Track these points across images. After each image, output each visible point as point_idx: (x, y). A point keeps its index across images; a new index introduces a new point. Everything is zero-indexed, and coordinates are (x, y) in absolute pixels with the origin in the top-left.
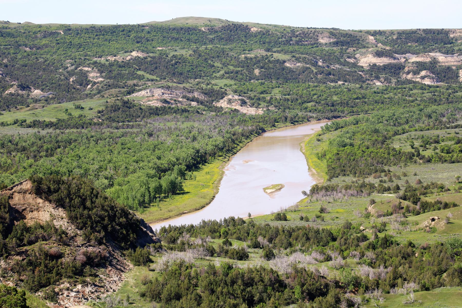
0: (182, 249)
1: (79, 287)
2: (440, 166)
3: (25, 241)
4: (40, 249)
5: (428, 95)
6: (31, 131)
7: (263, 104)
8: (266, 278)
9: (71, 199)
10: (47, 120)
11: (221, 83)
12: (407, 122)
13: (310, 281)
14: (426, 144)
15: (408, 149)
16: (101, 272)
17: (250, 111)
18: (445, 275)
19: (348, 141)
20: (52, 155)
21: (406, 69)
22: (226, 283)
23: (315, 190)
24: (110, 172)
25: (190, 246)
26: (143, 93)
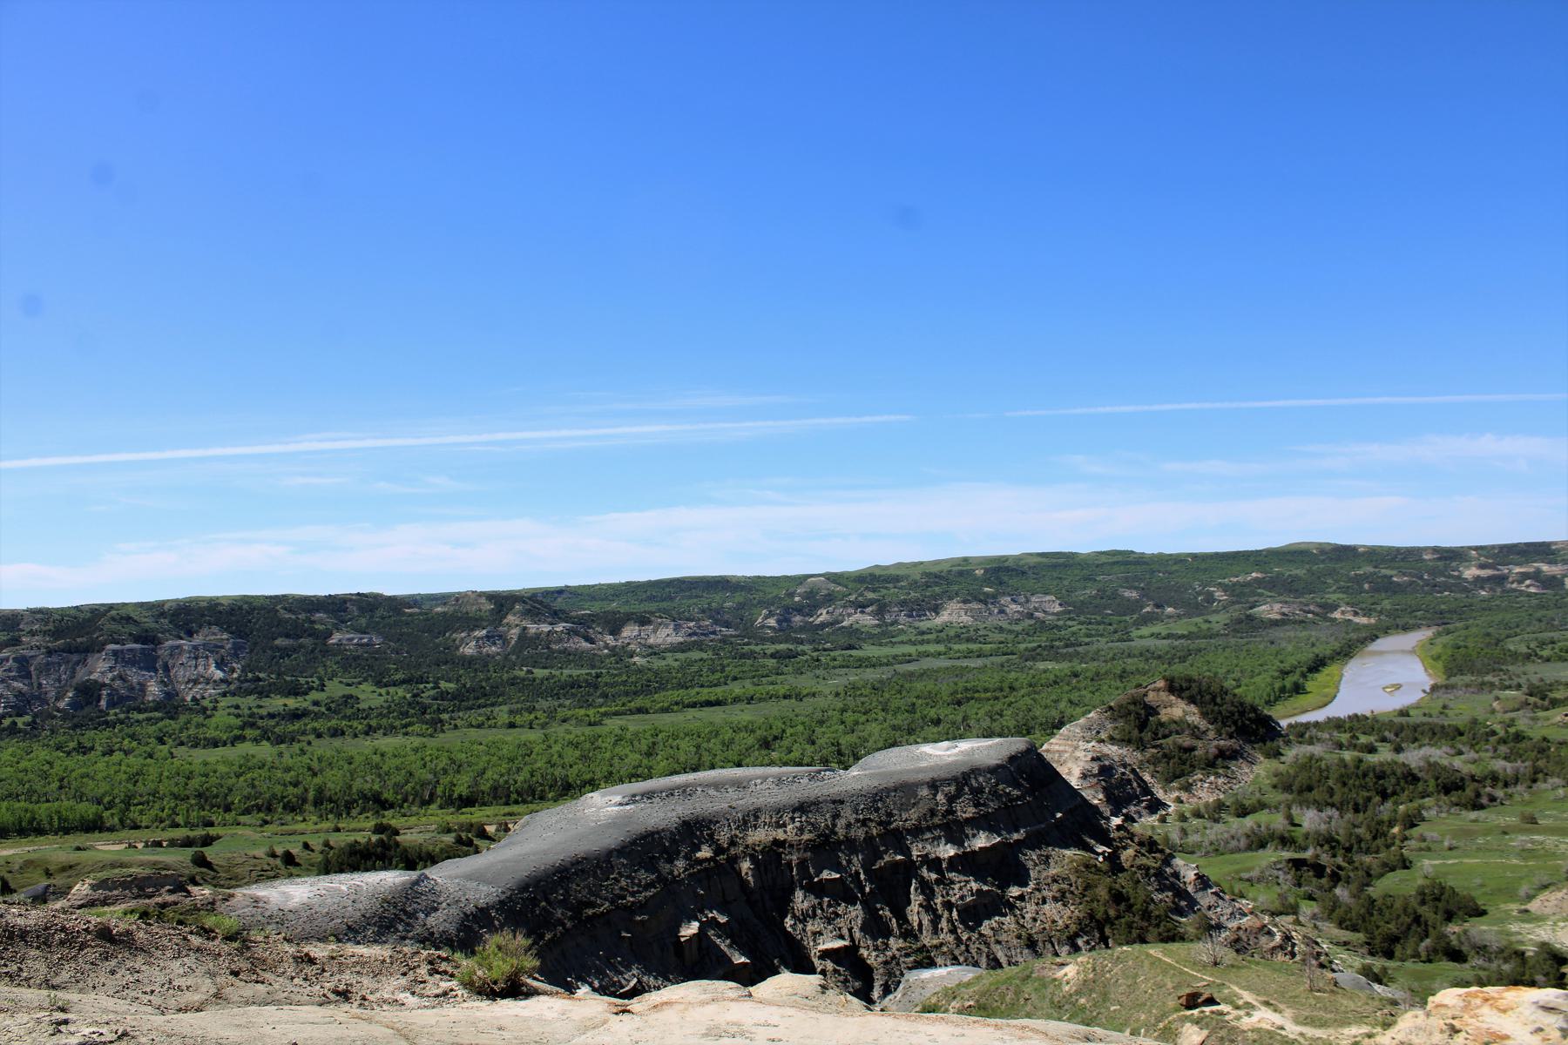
0: (1311, 742)
1: (1212, 778)
2: (1560, 665)
3: (1160, 736)
4: (1175, 743)
5: (1534, 602)
6: (1165, 641)
7: (1374, 614)
8: (1399, 772)
9: (1202, 697)
10: (1180, 632)
11: (1334, 597)
12: (1518, 626)
13: (1444, 775)
14: (1542, 644)
15: (1523, 649)
16: (1233, 765)
17: (1363, 620)
19: (1462, 644)
20: (1184, 662)
21: (1510, 579)
22: (1357, 776)
23: (1434, 688)
24: (1237, 675)
25: (1318, 740)
26: (1264, 607)
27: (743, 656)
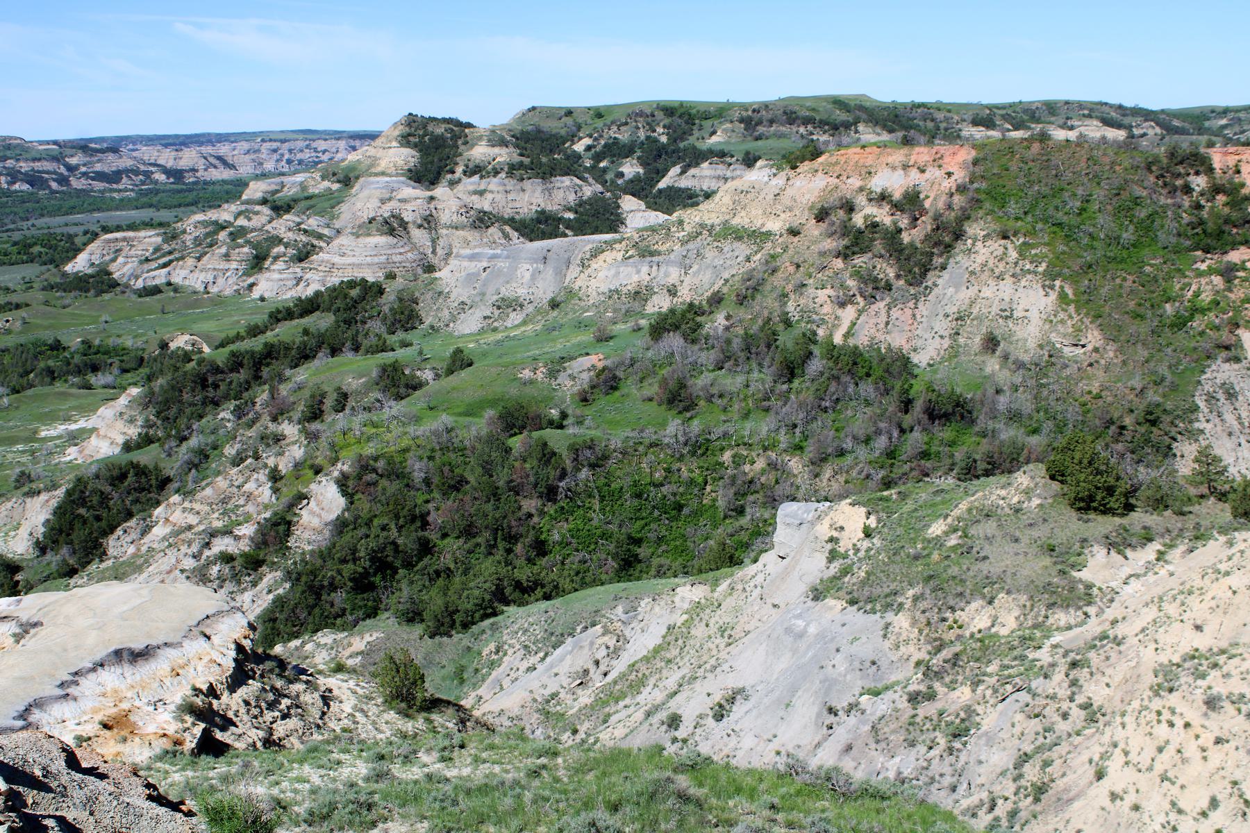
18: (32, 375)
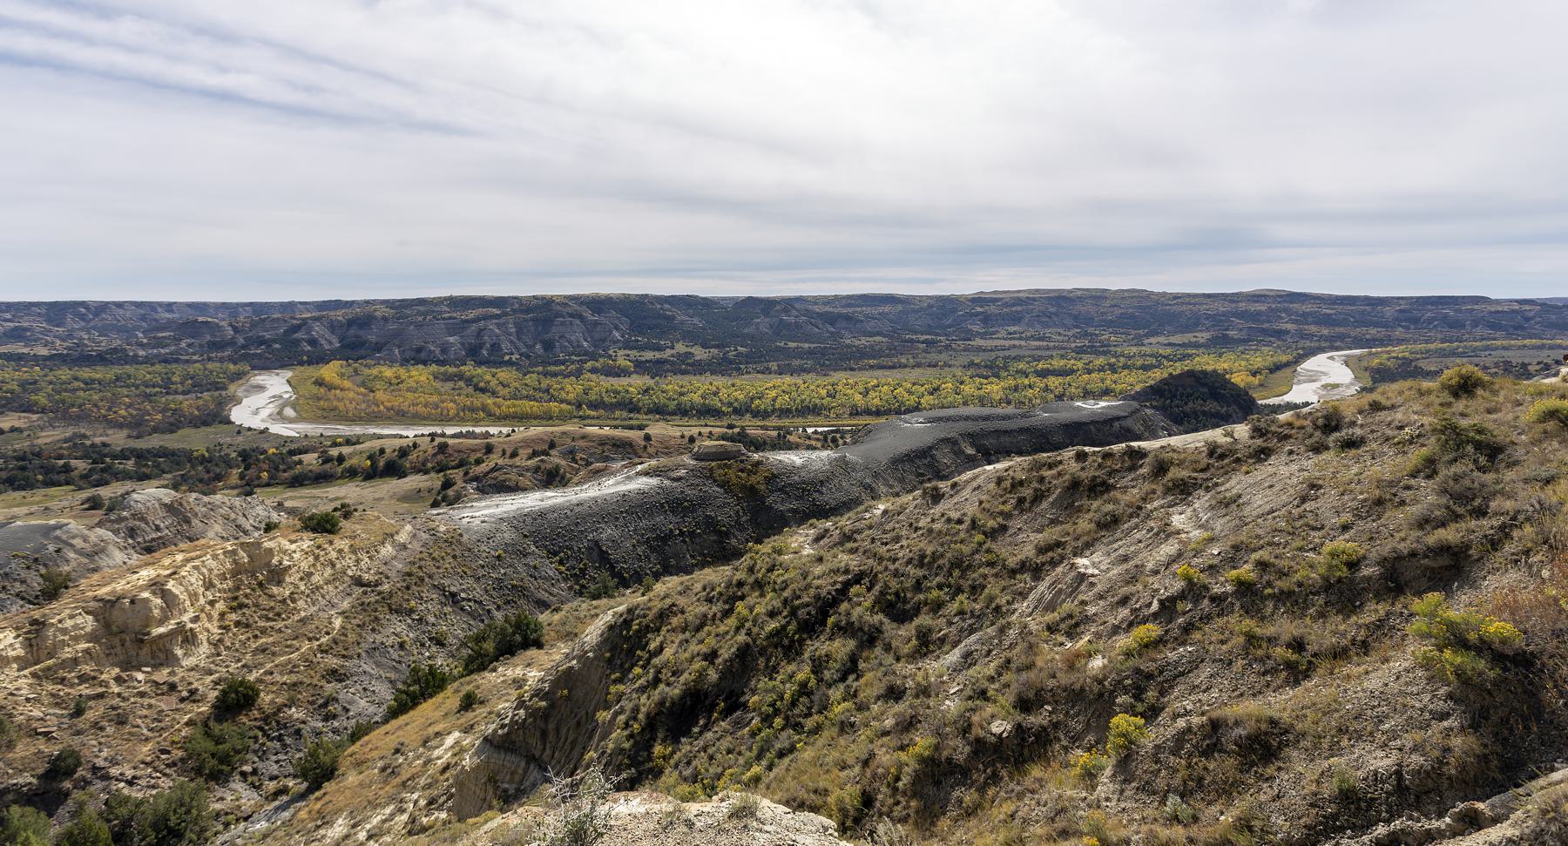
27: (906, 341)
